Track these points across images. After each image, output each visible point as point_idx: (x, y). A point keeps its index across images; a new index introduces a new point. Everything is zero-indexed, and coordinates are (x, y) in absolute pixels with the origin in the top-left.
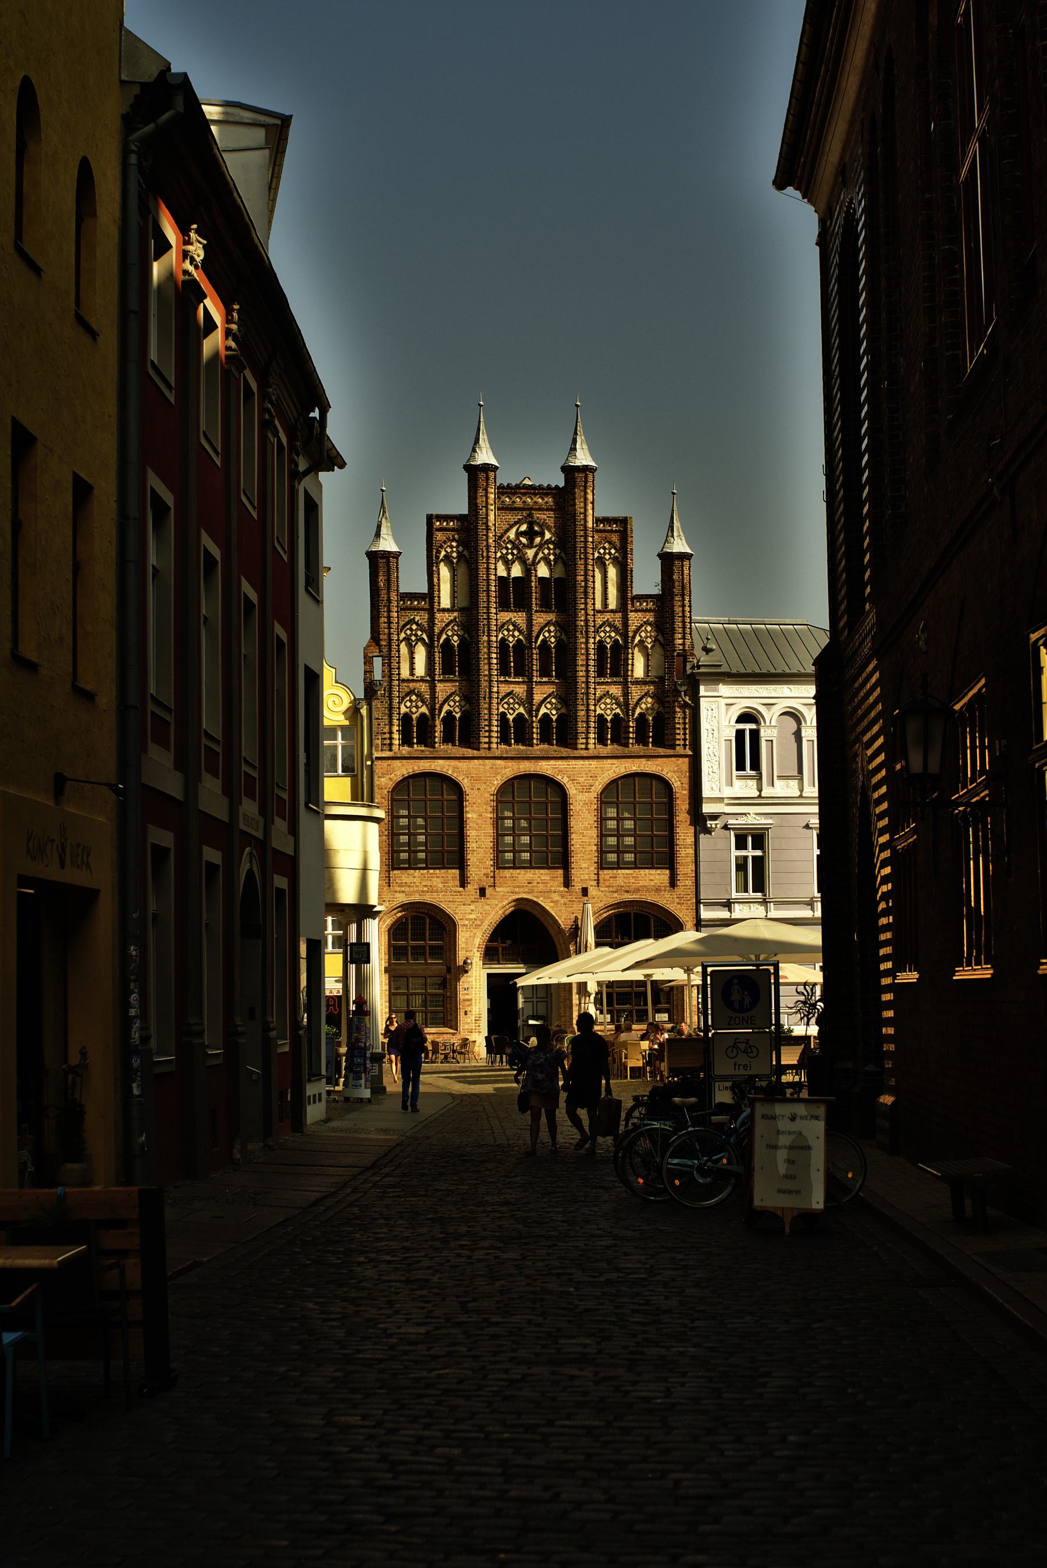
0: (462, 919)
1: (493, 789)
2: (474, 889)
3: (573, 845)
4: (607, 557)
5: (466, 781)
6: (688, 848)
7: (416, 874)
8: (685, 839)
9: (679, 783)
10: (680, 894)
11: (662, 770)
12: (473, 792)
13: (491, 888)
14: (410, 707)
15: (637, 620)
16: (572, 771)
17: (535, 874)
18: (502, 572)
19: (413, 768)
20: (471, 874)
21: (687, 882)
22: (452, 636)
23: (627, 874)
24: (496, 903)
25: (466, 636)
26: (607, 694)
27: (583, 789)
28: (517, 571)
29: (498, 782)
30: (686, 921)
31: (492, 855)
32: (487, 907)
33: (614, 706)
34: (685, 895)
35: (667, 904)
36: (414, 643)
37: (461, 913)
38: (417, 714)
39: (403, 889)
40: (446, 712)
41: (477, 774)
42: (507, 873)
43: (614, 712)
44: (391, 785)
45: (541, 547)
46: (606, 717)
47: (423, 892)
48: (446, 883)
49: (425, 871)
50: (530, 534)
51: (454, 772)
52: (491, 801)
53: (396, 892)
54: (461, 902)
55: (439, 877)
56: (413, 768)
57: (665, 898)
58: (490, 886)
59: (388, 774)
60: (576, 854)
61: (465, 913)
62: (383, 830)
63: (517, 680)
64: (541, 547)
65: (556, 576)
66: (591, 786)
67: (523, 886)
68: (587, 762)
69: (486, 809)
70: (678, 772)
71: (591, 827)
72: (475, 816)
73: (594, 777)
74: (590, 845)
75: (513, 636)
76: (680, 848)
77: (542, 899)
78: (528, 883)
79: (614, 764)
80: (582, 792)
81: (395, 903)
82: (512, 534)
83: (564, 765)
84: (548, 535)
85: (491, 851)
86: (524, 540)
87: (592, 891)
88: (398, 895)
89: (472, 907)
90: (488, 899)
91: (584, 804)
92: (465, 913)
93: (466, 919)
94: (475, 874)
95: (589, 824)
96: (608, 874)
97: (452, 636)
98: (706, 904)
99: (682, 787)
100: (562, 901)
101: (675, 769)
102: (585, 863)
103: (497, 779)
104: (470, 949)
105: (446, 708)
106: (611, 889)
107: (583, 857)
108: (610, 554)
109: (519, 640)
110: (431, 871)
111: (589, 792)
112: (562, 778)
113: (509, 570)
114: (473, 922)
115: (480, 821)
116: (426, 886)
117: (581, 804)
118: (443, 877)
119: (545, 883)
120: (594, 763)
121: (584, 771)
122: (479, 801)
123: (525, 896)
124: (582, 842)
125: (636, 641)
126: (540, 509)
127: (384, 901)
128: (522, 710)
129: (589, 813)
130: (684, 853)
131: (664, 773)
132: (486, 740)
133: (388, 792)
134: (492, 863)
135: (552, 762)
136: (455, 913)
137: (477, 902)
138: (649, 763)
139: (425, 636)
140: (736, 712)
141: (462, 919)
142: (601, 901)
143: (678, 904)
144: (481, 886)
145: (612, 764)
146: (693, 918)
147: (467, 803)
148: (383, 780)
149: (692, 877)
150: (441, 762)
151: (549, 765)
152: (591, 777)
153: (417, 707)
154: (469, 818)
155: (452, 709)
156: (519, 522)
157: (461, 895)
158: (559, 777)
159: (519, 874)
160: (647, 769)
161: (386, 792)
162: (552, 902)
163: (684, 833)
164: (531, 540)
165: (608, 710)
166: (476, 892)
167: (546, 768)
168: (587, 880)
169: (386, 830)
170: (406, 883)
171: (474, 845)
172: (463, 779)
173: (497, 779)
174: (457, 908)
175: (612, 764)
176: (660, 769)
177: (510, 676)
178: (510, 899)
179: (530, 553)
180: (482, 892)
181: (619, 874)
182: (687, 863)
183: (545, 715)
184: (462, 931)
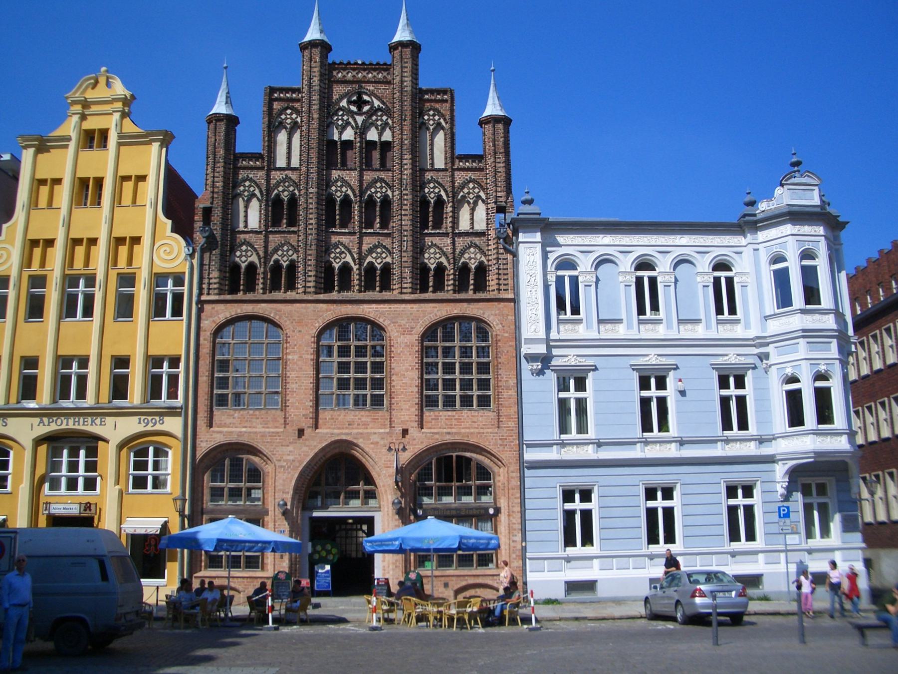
0: (280, 461)
1: (314, 331)
2: (293, 430)
3: (394, 386)
4: (431, 122)
5: (288, 322)
6: (511, 390)
7: (236, 415)
8: (507, 380)
9: (500, 326)
10: (502, 436)
11: (484, 314)
12: (294, 334)
13: (310, 430)
14: (241, 256)
15: (459, 178)
16: (393, 314)
17: (356, 416)
19: (236, 311)
20: (291, 415)
21: (509, 423)
22: (284, 191)
23: (449, 416)
24: (315, 444)
25: (296, 192)
27: (404, 331)
28: (349, 134)
29: (319, 324)
30: (509, 463)
31: (312, 396)
32: (305, 449)
33: (438, 256)
34: (508, 436)
35: (490, 445)
36: (246, 198)
37: (279, 455)
38: (246, 263)
39: (221, 429)
40: (274, 261)
41: (298, 317)
43: (437, 261)
44: (214, 327)
45: (370, 114)
46: (430, 265)
47: (241, 432)
48: (266, 424)
49: (245, 412)
50: (360, 103)
51: (276, 314)
52: (312, 343)
53: (213, 432)
54: (279, 442)
55: (258, 418)
56: (236, 311)
57: (487, 439)
58: (309, 427)
59: (211, 317)
60: (397, 395)
61: (283, 455)
62: (205, 371)
63: (343, 231)
64: (370, 114)
65: (383, 139)
66: (412, 328)
67: (343, 428)
68: (409, 306)
69: (307, 351)
70: (499, 315)
71: (412, 369)
72: (296, 357)
73: (416, 319)
74: (411, 386)
75: (341, 192)
76: (503, 389)
77: (361, 440)
78: (349, 425)
79: (436, 307)
80: (403, 334)
81: (213, 443)
82: (344, 103)
83: (385, 308)
85: (311, 392)
86: (353, 108)
87: (414, 432)
88: (215, 435)
89: (291, 448)
90: (306, 440)
91: (406, 346)
92: (283, 455)
93: (284, 461)
94: (295, 415)
95: (410, 366)
96: (430, 416)
97: (284, 191)
98: (528, 446)
99: (504, 330)
100: (382, 442)
101: (497, 312)
102: (405, 404)
103: (318, 322)
104: (287, 490)
105: (275, 257)
106: (432, 430)
107: (404, 398)
108: (434, 120)
109: (347, 196)
110: (251, 412)
111: (410, 334)
112: (384, 321)
113: (341, 133)
114: (291, 464)
115: (299, 363)
116: (245, 427)
117: (403, 346)
118: (262, 418)
119: (366, 425)
120: (416, 306)
121: (406, 314)
122: (300, 342)
123: (344, 437)
124: (403, 383)
125: (459, 197)
126: (369, 82)
127: (202, 441)
128: (349, 259)
129: (410, 354)
131: (485, 316)
132: (308, 284)
133: (211, 334)
134: (311, 404)
135: (374, 306)
136: (273, 454)
137: (296, 443)
138: (471, 306)
139: (257, 192)
141: (280, 461)
142: (422, 443)
143: (501, 445)
144: (300, 427)
145: (433, 307)
146: (517, 460)
147: (288, 345)
148: (206, 322)
149: (515, 418)
150: (263, 305)
151: (370, 308)
152: (413, 320)
153: (246, 256)
154: (289, 359)
155: (280, 258)
157: (280, 436)
158: (381, 320)
159: (339, 415)
160: (468, 312)
161: (209, 334)
162: (372, 443)
163: (506, 375)
164: (360, 108)
166: (295, 433)
168: (408, 421)
169: (207, 371)
170: (225, 423)
171: (294, 386)
172: (286, 321)
173: (318, 322)
174: (275, 449)
175: (433, 307)
176: (482, 312)
177: (335, 227)
178: (329, 441)
179: (360, 119)
180: (301, 432)
181: (441, 416)
182: (509, 404)
183: (371, 263)
184: (279, 472)
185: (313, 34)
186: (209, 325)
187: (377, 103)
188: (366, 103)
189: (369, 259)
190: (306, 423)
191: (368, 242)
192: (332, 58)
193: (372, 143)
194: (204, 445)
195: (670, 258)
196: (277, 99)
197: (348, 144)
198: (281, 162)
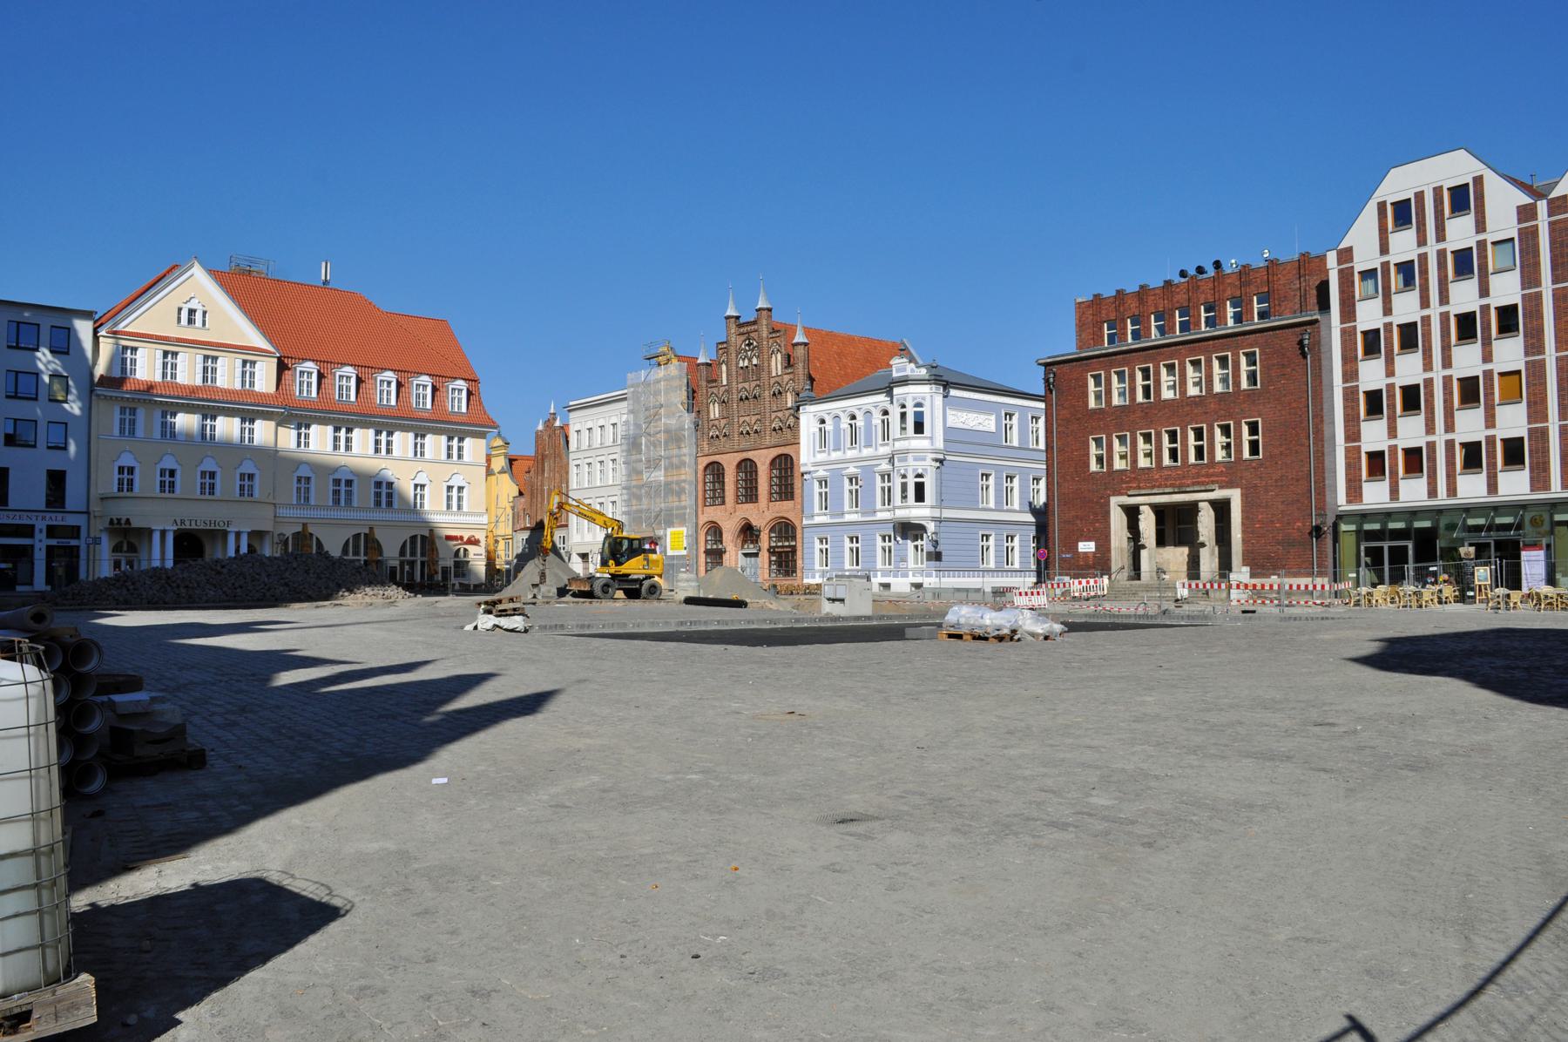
18: (741, 364)
26: (777, 417)
29: (735, 464)
42: (740, 505)
45: (753, 350)
73: (766, 457)
82: (743, 346)
84: (755, 343)
130: (797, 492)
140: (817, 418)
150: (717, 456)
156: (745, 340)
165: (776, 424)
167: (750, 455)
179: (749, 353)
185: (731, 312)
186: (701, 467)
187: (755, 343)
188: (752, 344)
189: (755, 428)
190: (732, 511)
191: (754, 419)
192: (742, 320)
193: (756, 365)
194: (701, 523)
195: (863, 411)
196: (721, 349)
197: (747, 367)
198: (725, 383)
